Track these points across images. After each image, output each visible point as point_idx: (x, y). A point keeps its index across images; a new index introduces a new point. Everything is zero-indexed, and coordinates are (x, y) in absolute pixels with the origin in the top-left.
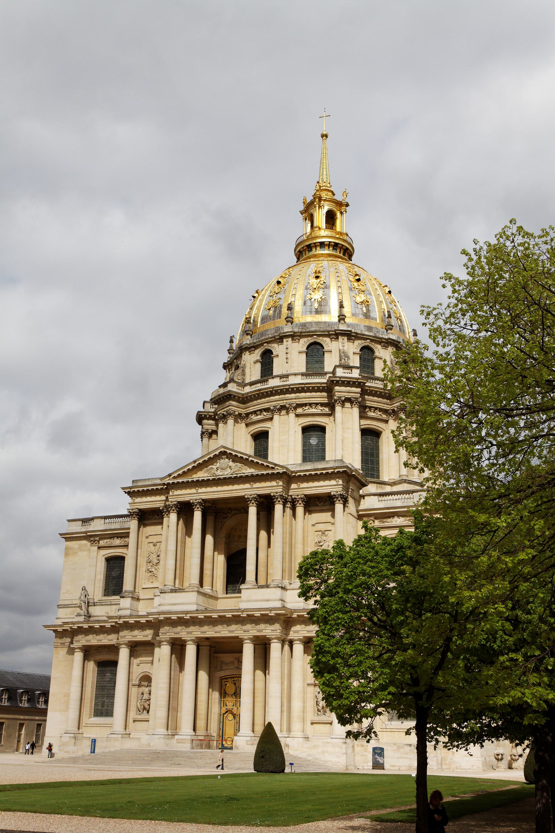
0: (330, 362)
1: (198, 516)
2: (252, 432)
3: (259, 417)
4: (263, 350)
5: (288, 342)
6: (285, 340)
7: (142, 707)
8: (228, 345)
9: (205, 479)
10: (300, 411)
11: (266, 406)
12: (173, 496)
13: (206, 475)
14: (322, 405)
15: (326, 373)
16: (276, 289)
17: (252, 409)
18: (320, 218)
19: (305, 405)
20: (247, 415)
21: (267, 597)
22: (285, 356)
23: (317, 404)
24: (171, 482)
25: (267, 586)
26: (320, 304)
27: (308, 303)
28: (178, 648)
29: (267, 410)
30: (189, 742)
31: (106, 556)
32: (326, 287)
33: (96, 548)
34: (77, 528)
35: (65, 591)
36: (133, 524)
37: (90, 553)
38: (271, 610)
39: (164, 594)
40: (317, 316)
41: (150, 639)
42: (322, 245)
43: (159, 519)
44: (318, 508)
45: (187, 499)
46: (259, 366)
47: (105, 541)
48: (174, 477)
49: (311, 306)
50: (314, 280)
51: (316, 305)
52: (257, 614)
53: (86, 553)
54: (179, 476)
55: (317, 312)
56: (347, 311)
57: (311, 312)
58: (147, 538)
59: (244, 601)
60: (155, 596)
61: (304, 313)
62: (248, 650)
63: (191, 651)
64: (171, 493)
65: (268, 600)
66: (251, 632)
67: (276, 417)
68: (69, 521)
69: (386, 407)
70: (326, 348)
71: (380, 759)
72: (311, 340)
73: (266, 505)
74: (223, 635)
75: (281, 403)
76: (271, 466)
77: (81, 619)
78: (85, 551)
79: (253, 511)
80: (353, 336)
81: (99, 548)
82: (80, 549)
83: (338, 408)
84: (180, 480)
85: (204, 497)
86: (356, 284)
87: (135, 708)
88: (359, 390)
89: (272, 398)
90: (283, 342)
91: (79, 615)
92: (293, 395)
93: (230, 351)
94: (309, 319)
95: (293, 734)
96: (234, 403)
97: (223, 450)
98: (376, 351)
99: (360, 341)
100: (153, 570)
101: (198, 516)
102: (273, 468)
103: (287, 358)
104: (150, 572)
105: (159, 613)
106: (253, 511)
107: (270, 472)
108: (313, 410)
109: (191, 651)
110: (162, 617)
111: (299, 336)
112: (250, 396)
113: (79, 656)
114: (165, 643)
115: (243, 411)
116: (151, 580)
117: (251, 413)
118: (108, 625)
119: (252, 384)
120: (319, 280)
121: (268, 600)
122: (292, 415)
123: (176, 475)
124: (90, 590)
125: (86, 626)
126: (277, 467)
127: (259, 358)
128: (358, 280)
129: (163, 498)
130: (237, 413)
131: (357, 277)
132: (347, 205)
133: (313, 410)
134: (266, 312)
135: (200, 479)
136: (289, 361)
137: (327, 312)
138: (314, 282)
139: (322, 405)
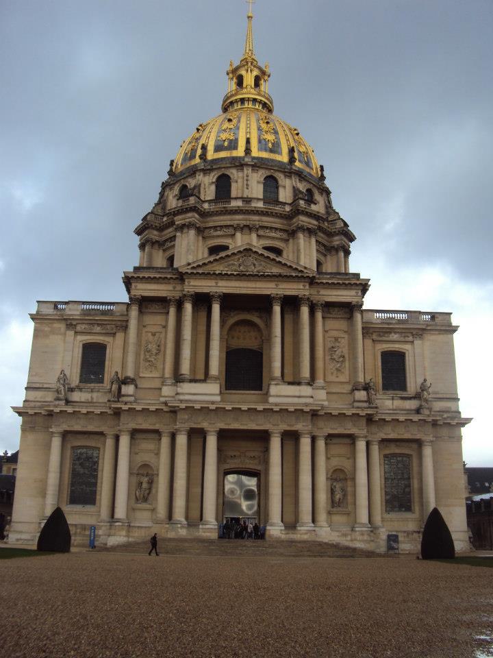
0: (285, 195)
1: (216, 308)
2: (210, 246)
3: (219, 233)
4: (219, 174)
5: (248, 171)
6: (245, 169)
7: (142, 496)
8: (168, 168)
9: (229, 273)
10: (261, 232)
11: (229, 223)
12: (190, 286)
13: (227, 269)
14: (281, 230)
15: (284, 204)
16: (226, 125)
17: (211, 224)
18: (249, 79)
19: (267, 228)
20: (206, 228)
21: (297, 394)
22: (245, 182)
23: (276, 229)
24: (189, 271)
25: (299, 384)
26: (273, 144)
27: (263, 142)
28: (197, 436)
29: (227, 226)
30: (191, 529)
31: (85, 342)
32: (276, 133)
33: (72, 333)
34: (49, 310)
35: (34, 373)
36: (134, 312)
37: (65, 337)
38: (307, 405)
39: (181, 384)
40: (272, 154)
41: (157, 428)
42: (255, 100)
43: (159, 309)
44: (331, 316)
45: (206, 290)
46: (213, 188)
47: (83, 326)
48: (193, 268)
49: (266, 144)
50: (265, 125)
51: (270, 145)
52: (291, 409)
53: (60, 337)
54: (199, 266)
55: (271, 151)
56: (296, 155)
57: (266, 151)
58: (144, 326)
59: (273, 396)
60: (163, 385)
61: (260, 149)
62: (275, 444)
63: (212, 442)
64: (186, 283)
65: (299, 397)
66: (281, 426)
67: (238, 235)
68: (38, 302)
69: (326, 243)
70: (280, 182)
71: (395, 545)
72: (268, 173)
73: (291, 304)
74: (249, 428)
75: (245, 223)
76: (300, 268)
77: (63, 403)
78: (57, 334)
79: (277, 309)
80: (303, 178)
81: (76, 332)
82: (53, 332)
83: (301, 235)
84: (200, 271)
85: (225, 291)
86: (296, 137)
87: (134, 497)
88: (315, 222)
89: (237, 217)
90: (243, 169)
91: (58, 399)
92: (256, 218)
93: (171, 173)
94: (265, 155)
95: (319, 524)
96: (196, 216)
97: (248, 247)
98: (315, 195)
99: (305, 184)
100: (153, 360)
101: (216, 308)
102: (301, 271)
103: (247, 185)
104: (149, 361)
105: (181, 401)
106: (277, 309)
107: (300, 275)
108: (273, 234)
109: (212, 442)
110: (183, 406)
111: (259, 167)
112: (213, 212)
113: (56, 442)
114: (166, 434)
115: (203, 225)
116: (150, 370)
117: (210, 228)
118: (98, 411)
119: (209, 202)
120: (269, 125)
121: (299, 397)
122: (254, 236)
123: (195, 265)
124: (67, 373)
125: (70, 410)
126: (305, 271)
127: (214, 180)
128: (298, 134)
129: (170, 287)
130: (198, 226)
131: (296, 132)
132: (269, 76)
133: (273, 234)
134: (220, 143)
135: (223, 273)
136: (249, 187)
137: (280, 153)
138: (264, 126)
139: (281, 230)
